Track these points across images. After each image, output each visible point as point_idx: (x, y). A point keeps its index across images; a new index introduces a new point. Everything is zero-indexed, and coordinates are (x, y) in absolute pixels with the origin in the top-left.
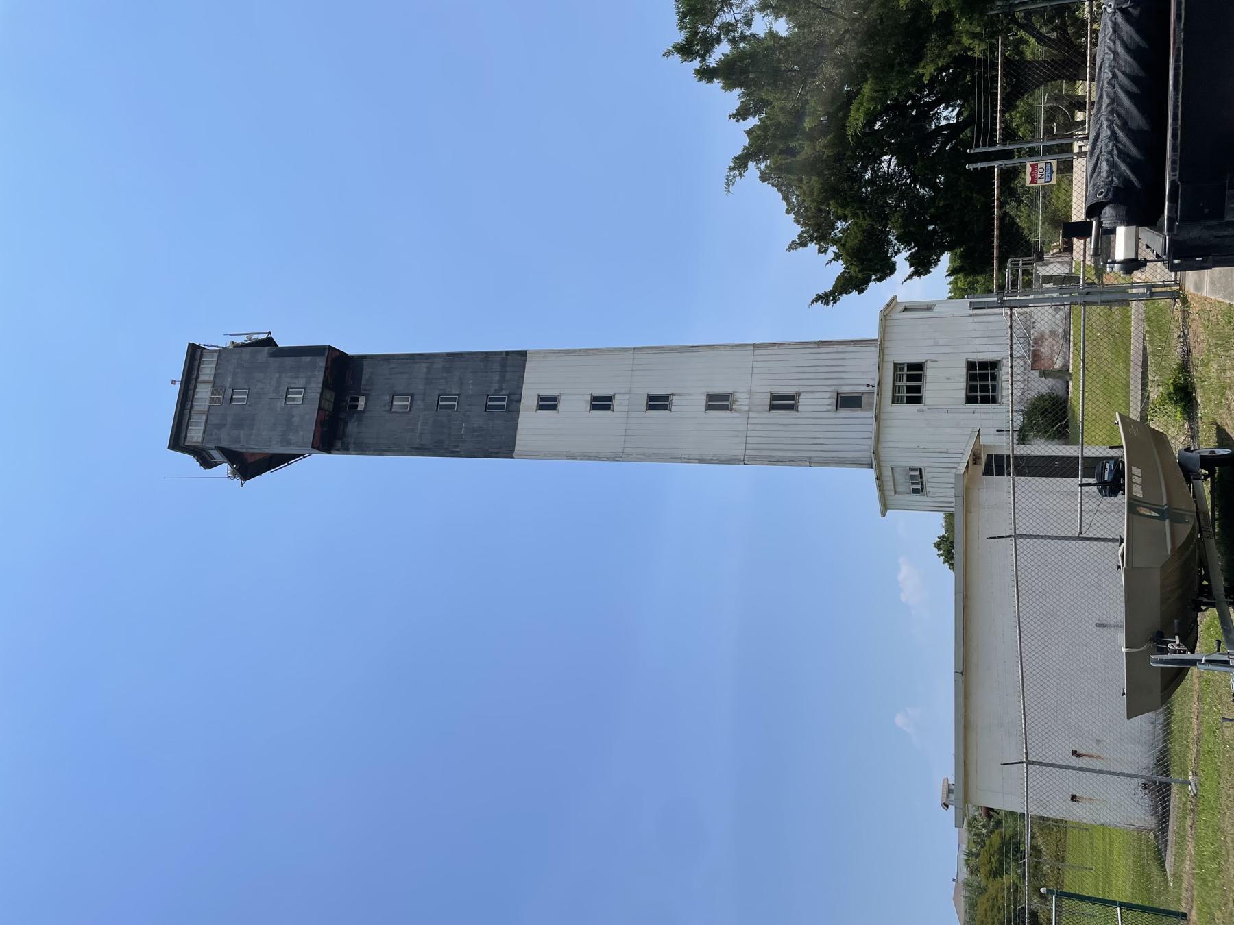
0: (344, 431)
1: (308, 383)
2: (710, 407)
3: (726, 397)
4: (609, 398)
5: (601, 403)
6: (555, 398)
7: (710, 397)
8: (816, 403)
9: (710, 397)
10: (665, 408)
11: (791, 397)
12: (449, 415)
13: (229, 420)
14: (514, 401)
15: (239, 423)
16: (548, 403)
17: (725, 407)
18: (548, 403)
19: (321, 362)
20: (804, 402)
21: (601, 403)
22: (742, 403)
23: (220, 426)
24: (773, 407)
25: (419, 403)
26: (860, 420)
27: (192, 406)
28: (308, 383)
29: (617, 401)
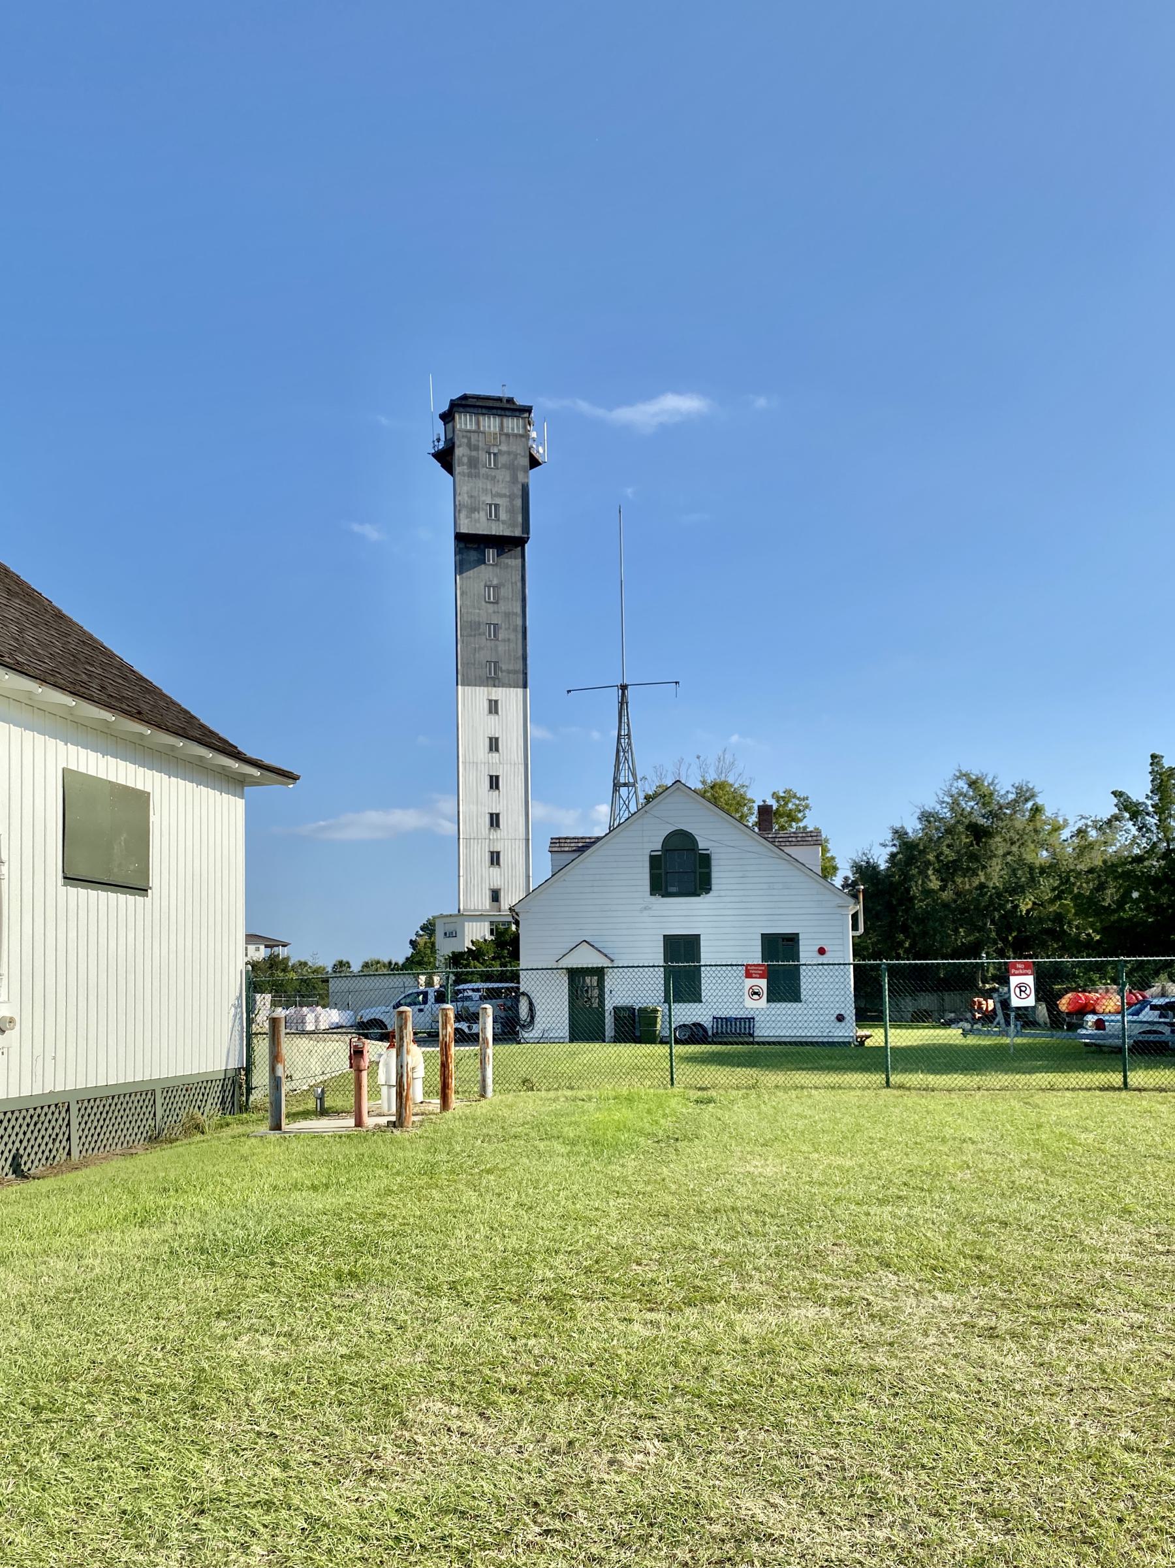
0: (468, 548)
1: (504, 522)
2: (491, 815)
3: (498, 825)
4: (497, 750)
5: (494, 745)
6: (497, 712)
7: (498, 815)
8: (495, 877)
9: (498, 815)
10: (491, 787)
11: (498, 864)
12: (484, 634)
13: (474, 453)
14: (493, 680)
15: (473, 463)
16: (493, 707)
17: (492, 825)
18: (493, 707)
19: (518, 533)
20: (495, 871)
21: (494, 745)
22: (494, 835)
23: (469, 445)
24: (492, 853)
25: (491, 608)
26: (486, 903)
27: (484, 414)
28: (504, 522)
29: (495, 755)
